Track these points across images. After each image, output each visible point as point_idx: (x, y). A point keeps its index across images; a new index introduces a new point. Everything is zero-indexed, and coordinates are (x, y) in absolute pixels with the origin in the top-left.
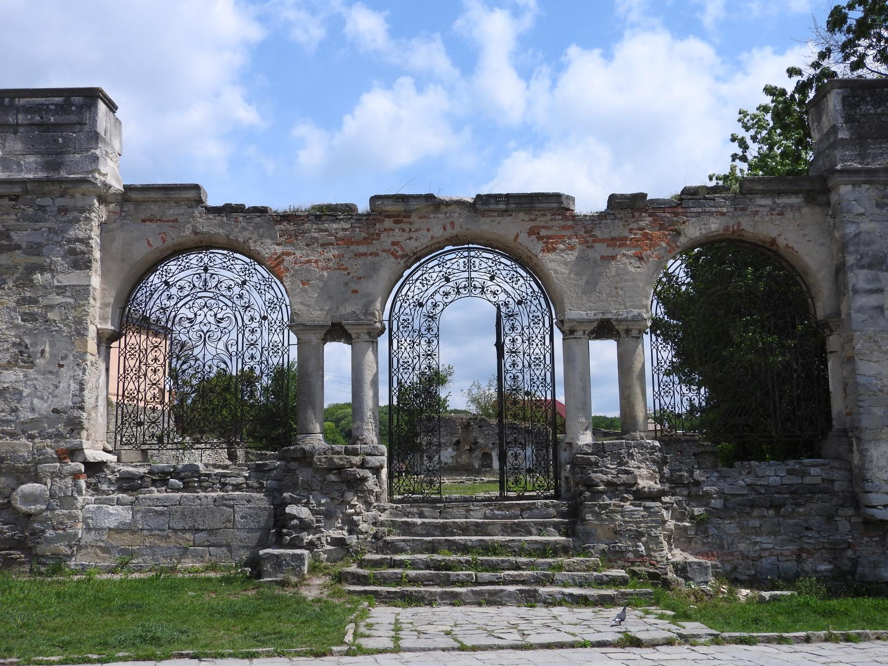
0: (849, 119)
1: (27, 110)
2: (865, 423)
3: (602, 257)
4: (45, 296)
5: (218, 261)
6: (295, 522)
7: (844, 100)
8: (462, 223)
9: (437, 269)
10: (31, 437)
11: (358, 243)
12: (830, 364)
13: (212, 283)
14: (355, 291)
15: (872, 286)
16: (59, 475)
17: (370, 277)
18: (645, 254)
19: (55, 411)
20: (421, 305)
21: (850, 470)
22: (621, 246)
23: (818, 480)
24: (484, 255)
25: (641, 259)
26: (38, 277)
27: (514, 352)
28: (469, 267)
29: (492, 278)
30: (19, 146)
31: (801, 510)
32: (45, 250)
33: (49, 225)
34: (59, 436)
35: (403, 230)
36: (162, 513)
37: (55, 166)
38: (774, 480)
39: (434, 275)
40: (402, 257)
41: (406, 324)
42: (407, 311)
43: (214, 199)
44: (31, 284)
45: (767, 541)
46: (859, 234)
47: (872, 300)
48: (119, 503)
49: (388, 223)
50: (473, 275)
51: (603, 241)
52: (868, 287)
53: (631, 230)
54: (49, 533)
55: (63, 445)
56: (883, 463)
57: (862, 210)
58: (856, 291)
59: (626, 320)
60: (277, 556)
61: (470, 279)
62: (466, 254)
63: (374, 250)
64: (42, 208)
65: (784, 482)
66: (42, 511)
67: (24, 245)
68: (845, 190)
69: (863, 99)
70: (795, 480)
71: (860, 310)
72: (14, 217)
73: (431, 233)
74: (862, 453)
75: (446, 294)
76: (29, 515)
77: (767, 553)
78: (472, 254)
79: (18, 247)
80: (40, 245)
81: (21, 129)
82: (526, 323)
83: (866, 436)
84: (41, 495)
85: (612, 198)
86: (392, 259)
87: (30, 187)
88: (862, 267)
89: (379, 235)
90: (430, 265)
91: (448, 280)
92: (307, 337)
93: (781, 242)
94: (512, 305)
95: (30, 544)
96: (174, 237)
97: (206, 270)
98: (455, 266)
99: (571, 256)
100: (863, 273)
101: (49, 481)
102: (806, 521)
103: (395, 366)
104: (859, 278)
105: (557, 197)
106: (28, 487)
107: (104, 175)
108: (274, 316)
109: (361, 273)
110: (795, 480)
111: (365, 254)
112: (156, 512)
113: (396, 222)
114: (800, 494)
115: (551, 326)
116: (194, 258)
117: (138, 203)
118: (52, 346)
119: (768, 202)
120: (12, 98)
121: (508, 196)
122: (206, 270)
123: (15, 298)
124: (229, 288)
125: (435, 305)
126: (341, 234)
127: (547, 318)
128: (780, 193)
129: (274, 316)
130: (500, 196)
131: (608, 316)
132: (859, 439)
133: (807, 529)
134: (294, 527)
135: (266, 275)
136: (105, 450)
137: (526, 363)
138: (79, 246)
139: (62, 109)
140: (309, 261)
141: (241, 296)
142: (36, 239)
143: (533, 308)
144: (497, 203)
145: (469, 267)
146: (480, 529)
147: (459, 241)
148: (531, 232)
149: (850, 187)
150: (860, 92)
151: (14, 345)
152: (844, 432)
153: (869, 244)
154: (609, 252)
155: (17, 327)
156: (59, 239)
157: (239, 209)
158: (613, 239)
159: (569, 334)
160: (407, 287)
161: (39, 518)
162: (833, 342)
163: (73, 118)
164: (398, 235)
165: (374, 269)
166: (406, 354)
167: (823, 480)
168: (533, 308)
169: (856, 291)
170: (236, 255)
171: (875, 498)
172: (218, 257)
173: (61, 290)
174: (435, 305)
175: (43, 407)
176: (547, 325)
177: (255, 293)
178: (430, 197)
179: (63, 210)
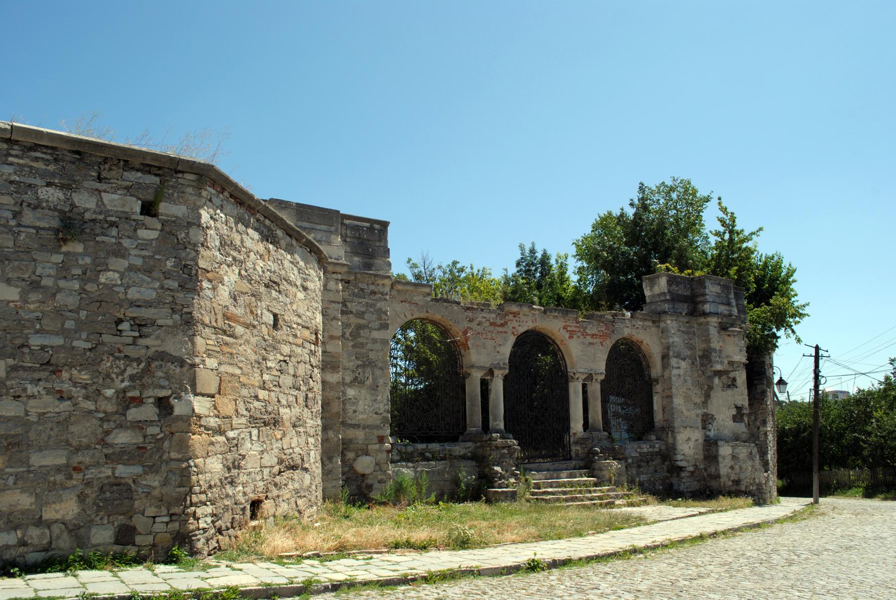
2: (676, 424)
4: (367, 343)
11: (499, 326)
12: (655, 399)
16: (380, 451)
32: (366, 316)
33: (366, 300)
34: (377, 427)
38: (645, 450)
44: (359, 335)
48: (408, 467)
49: (511, 317)
54: (376, 485)
64: (362, 290)
67: (354, 311)
74: (674, 438)
76: (363, 475)
79: (352, 313)
80: (364, 313)
83: (676, 430)
104: (674, 361)
123: (351, 343)
126: (492, 321)
128: (645, 320)
132: (673, 432)
148: (564, 328)
152: (663, 429)
154: (591, 340)
161: (371, 476)
162: (658, 388)
164: (515, 324)
165: (506, 340)
171: (679, 457)
173: (375, 341)
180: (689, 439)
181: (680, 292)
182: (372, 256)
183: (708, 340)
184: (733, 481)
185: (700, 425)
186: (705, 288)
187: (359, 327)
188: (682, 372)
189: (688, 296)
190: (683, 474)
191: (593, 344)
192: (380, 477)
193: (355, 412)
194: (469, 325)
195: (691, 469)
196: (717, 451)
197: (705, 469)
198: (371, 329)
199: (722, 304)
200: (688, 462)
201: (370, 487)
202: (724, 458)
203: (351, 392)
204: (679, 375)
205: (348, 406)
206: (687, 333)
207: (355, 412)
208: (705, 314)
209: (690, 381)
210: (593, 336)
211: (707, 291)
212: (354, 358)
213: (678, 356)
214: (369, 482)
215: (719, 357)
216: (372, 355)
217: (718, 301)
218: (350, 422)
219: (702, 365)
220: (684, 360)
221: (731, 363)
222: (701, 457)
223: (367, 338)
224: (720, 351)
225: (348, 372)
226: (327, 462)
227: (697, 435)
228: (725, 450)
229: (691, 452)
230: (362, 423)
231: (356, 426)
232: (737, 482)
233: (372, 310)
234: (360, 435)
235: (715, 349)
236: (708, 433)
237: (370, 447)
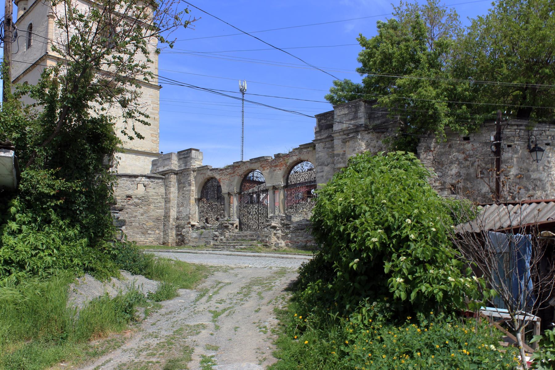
37: (186, 166)
99: (268, 171)
106: (184, 230)
117: (200, 170)
119: (306, 150)
188: (324, 174)
215: (342, 158)
220: (327, 165)
235: (338, 155)
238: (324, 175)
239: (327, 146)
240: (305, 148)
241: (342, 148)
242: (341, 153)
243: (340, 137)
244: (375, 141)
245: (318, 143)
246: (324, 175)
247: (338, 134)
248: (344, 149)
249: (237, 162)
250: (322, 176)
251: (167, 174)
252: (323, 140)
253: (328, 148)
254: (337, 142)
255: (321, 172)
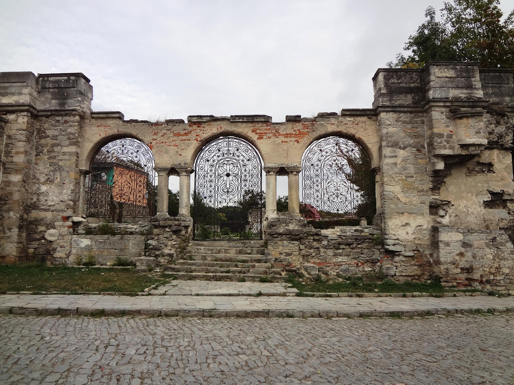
0: (386, 85)
1: (53, 82)
2: (386, 211)
3: (282, 142)
5: (128, 142)
6: (151, 247)
7: (384, 77)
8: (226, 127)
9: (215, 146)
10: (53, 211)
11: (182, 135)
13: (125, 152)
14: (181, 155)
15: (392, 155)
16: (64, 227)
17: (187, 149)
18: (300, 140)
19: (61, 201)
20: (208, 161)
21: (382, 230)
22: (290, 137)
23: (368, 234)
24: (235, 140)
25: (298, 142)
26: (56, 149)
27: (245, 180)
28: (229, 145)
29: (237, 150)
30: (50, 96)
31: (360, 246)
32: (59, 138)
35: (201, 130)
36: (101, 242)
39: (214, 149)
40: (200, 141)
41: (202, 169)
42: (203, 163)
43: (126, 119)
45: (345, 259)
46: (387, 133)
47: (392, 160)
50: (230, 148)
51: (283, 135)
52: (391, 155)
53: (294, 130)
54: (59, 249)
55: (66, 214)
56: (393, 227)
57: (390, 123)
58: (385, 157)
59: (291, 167)
60: (142, 260)
61: (229, 150)
62: (227, 140)
63: (189, 138)
64: (58, 121)
65: (353, 234)
66: (56, 241)
68: (383, 115)
69: (393, 77)
70: (358, 234)
71: (387, 164)
72: (47, 125)
73: (212, 131)
74: (385, 222)
75: (219, 156)
76: (51, 242)
77: (344, 263)
78: (230, 140)
79: (49, 136)
80: (57, 136)
81: (51, 90)
82: (251, 168)
84: (56, 234)
85: (287, 117)
86: (196, 142)
87: (53, 113)
88: (389, 146)
89: (191, 132)
90: (212, 144)
91: (219, 151)
92: (161, 174)
93: (357, 136)
94: (245, 161)
95: (52, 253)
96: (110, 132)
97: (123, 146)
98: (222, 145)
100: (389, 149)
101: (59, 229)
102: (362, 251)
103: (197, 185)
104: (387, 151)
105: (264, 116)
106: (52, 231)
107: (83, 108)
108: (149, 165)
109: (183, 148)
110: (358, 234)
111: (185, 140)
112: (99, 242)
113: (198, 127)
114: (359, 239)
115: (261, 170)
116: (118, 141)
118: (60, 176)
120: (48, 77)
121: (243, 116)
122: (123, 146)
124: (132, 153)
125: (214, 161)
127: (259, 167)
129: (149, 165)
130: (241, 116)
131: (284, 166)
132: (384, 218)
133: (362, 254)
134: (151, 249)
135: (147, 148)
136: (82, 217)
137: (250, 185)
138: (72, 136)
139: (67, 81)
140: (163, 142)
141: (136, 157)
142: (56, 133)
143: (254, 162)
144: (239, 119)
145: (229, 145)
146: (226, 251)
147: (226, 134)
149: (385, 113)
150: (391, 73)
151: (47, 175)
153: (391, 137)
154: (285, 139)
155: (48, 167)
156: (64, 133)
157: (136, 121)
158: (287, 134)
159: (268, 172)
160: (203, 153)
161: (56, 243)
162: (378, 178)
163: (71, 85)
166: (201, 181)
167: (370, 234)
168: (254, 162)
169: (385, 157)
170: (135, 140)
171: (389, 242)
172: (128, 141)
173: (64, 154)
174: (214, 161)
175: (56, 200)
176: (259, 169)
177: (142, 155)
178: (212, 116)
179: (66, 122)
180: (407, 224)
181: (403, 85)
182: (66, 98)
183: (431, 127)
184: (462, 269)
185: (428, 211)
186: (429, 74)
187: (53, 146)
188: (399, 160)
189: (415, 87)
190: (397, 259)
191: (287, 142)
192: (61, 244)
193: (46, 200)
194: (155, 137)
195: (411, 254)
196: (438, 237)
197: (431, 255)
198: (62, 146)
199: (458, 87)
200: (405, 246)
201: (55, 250)
202: (447, 244)
203: (44, 188)
204: (395, 164)
205: (41, 197)
206: (410, 122)
207: (46, 200)
208: (430, 101)
209: (412, 169)
210: (287, 135)
211: (432, 78)
212: (48, 166)
213: (395, 145)
214: (54, 246)
216: (61, 163)
217: (450, 85)
218: (43, 207)
219: (429, 152)
220: (404, 148)
221: (464, 146)
222: (428, 242)
223: (58, 152)
224: (450, 136)
225: (44, 175)
226: (7, 232)
227: (425, 221)
228: (450, 238)
229: (411, 237)
230: (52, 208)
231: (45, 210)
232: (469, 270)
233: (64, 133)
234: (49, 215)
235: (441, 135)
236: (439, 220)
237: (56, 223)
238: (399, 162)
239: (402, 119)
240: (350, 116)
241: (447, 126)
242: (445, 134)
243: (443, 109)
244: (493, 126)
245: (387, 112)
246: (399, 162)
247: (442, 104)
248: (450, 129)
249: (201, 117)
250: (395, 164)
251: (12, 112)
252: (398, 109)
253: (404, 122)
254: (438, 115)
255: (392, 157)
